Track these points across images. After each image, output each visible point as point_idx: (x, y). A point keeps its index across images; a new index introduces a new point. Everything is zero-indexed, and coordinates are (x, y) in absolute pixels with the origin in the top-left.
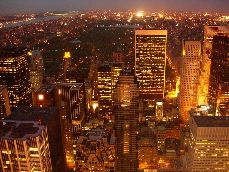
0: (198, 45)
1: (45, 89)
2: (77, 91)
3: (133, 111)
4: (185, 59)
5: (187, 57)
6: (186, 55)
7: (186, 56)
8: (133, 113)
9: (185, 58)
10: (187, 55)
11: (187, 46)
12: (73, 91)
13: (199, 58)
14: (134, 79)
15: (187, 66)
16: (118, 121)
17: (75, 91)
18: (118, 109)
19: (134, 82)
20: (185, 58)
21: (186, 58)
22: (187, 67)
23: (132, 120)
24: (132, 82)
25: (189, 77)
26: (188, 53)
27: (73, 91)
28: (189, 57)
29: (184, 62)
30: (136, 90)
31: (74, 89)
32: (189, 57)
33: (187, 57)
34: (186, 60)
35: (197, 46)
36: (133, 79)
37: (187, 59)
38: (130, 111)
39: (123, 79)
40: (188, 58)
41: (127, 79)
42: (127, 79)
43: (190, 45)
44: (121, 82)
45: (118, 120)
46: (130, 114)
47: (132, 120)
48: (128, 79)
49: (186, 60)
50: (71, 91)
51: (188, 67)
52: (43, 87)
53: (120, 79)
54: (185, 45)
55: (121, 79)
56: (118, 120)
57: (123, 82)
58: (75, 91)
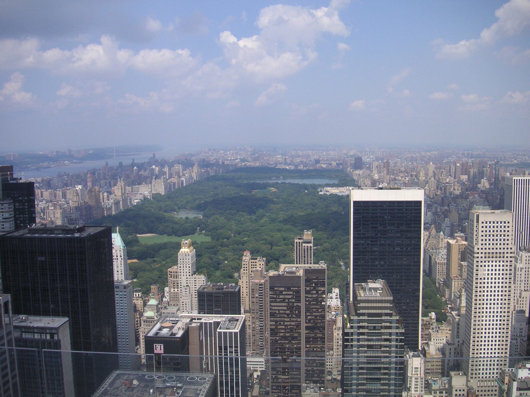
0: (508, 223)
1: (168, 329)
2: (236, 334)
3: (389, 380)
4: (480, 255)
5: (484, 251)
6: (482, 247)
7: (482, 249)
8: (389, 385)
9: (478, 253)
10: (484, 247)
11: (483, 225)
12: (225, 333)
13: (511, 253)
14: (391, 305)
15: (485, 270)
17: (231, 333)
18: (354, 376)
19: (391, 312)
20: (478, 253)
21: (482, 253)
22: (484, 274)
24: (388, 311)
25: (489, 298)
26: (486, 240)
27: (226, 333)
28: (487, 251)
29: (478, 262)
30: (397, 331)
31: (227, 329)
32: (489, 251)
33: (484, 251)
34: (482, 257)
35: (507, 225)
36: (388, 305)
37: (483, 255)
38: (382, 382)
39: (366, 305)
40: (485, 253)
43: (490, 223)
46: (382, 387)
48: (380, 305)
49: (482, 257)
50: (220, 333)
51: (487, 272)
52: (164, 325)
53: (358, 305)
54: (478, 221)
55: (362, 305)
58: (229, 332)
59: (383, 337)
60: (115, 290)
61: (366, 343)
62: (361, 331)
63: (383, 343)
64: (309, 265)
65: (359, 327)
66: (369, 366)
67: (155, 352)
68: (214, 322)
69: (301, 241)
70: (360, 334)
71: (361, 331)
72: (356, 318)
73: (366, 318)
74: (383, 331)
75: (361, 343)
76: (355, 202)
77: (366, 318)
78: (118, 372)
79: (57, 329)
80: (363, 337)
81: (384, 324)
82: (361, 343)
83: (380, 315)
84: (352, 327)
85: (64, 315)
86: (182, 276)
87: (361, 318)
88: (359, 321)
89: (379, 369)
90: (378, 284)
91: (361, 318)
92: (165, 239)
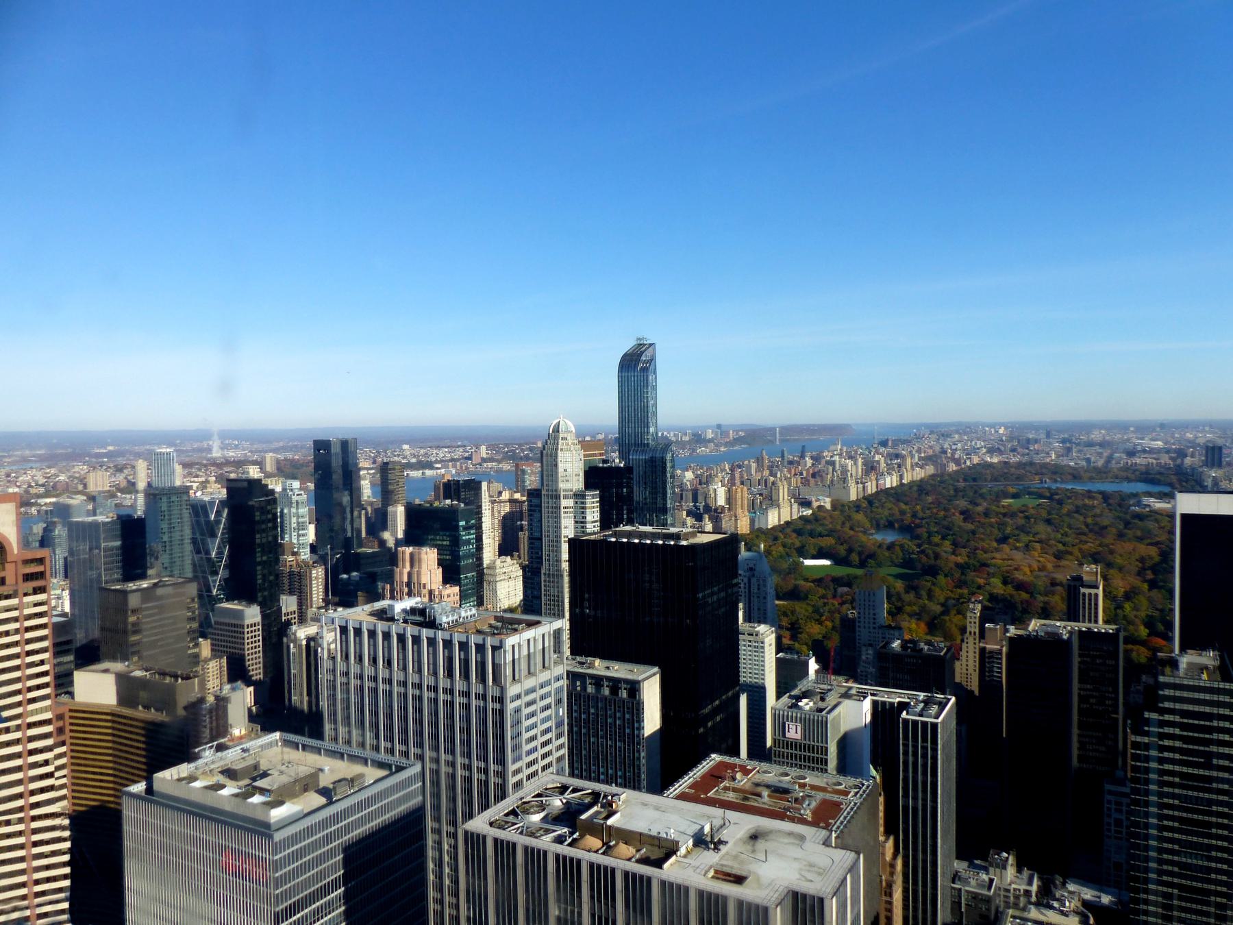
2: (934, 726)
12: (915, 723)
16: (1147, 891)
17: (925, 724)
23: (1224, 901)
39: (1178, 693)
41: (1196, 695)
42: (1196, 695)
44: (1166, 705)
45: (1151, 886)
47: (1224, 901)
48: (1208, 697)
50: (906, 721)
55: (1167, 692)
56: (1151, 886)
57: (1178, 706)
59: (1215, 761)
60: (741, 637)
61: (1177, 768)
62: (1166, 743)
63: (1215, 774)
64: (1087, 625)
65: (1162, 736)
66: (1185, 815)
67: (787, 735)
68: (899, 703)
69: (1078, 584)
70: (1162, 749)
71: (1166, 743)
72: (1154, 716)
73: (1178, 719)
74: (1214, 749)
75: (1166, 767)
76: (1184, 516)
77: (1178, 719)
78: (716, 758)
79: (638, 682)
80: (1171, 755)
81: (1215, 736)
82: (1166, 767)
83: (1210, 717)
84: (1147, 734)
85: (649, 662)
86: (862, 629)
87: (1167, 717)
88: (1162, 724)
89: (1210, 825)
90: (1209, 658)
91: (1167, 717)
92: (843, 571)
